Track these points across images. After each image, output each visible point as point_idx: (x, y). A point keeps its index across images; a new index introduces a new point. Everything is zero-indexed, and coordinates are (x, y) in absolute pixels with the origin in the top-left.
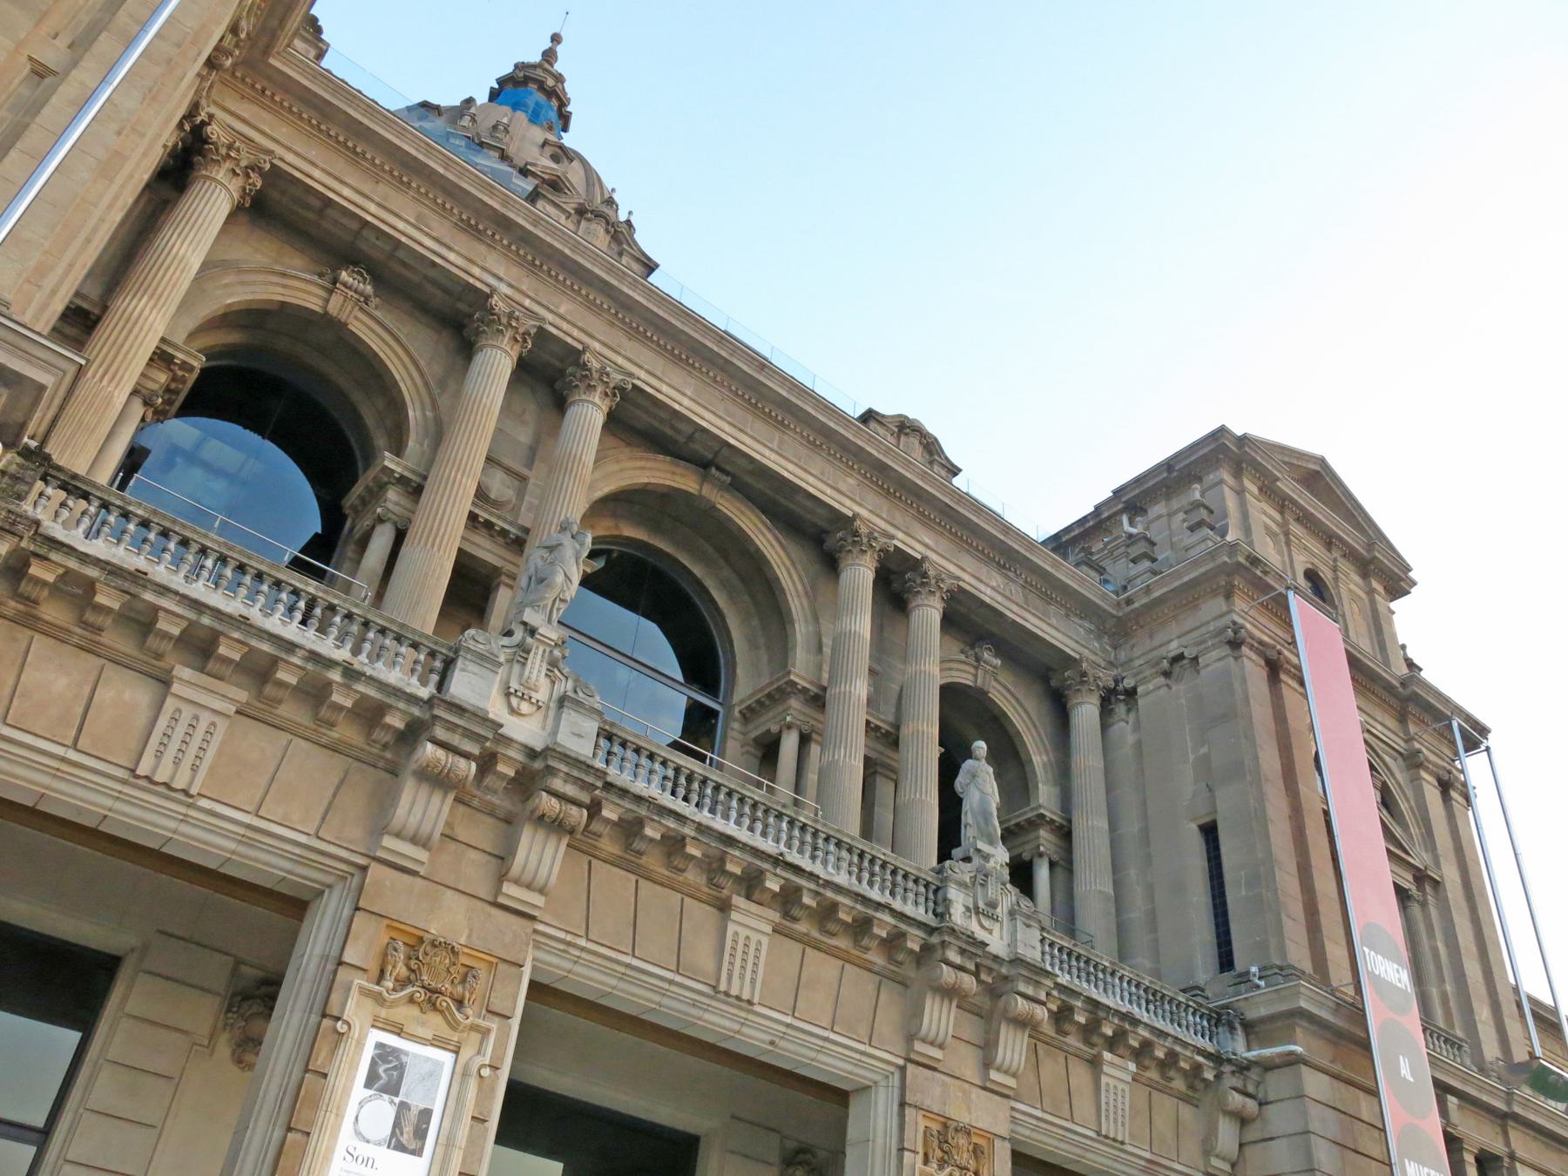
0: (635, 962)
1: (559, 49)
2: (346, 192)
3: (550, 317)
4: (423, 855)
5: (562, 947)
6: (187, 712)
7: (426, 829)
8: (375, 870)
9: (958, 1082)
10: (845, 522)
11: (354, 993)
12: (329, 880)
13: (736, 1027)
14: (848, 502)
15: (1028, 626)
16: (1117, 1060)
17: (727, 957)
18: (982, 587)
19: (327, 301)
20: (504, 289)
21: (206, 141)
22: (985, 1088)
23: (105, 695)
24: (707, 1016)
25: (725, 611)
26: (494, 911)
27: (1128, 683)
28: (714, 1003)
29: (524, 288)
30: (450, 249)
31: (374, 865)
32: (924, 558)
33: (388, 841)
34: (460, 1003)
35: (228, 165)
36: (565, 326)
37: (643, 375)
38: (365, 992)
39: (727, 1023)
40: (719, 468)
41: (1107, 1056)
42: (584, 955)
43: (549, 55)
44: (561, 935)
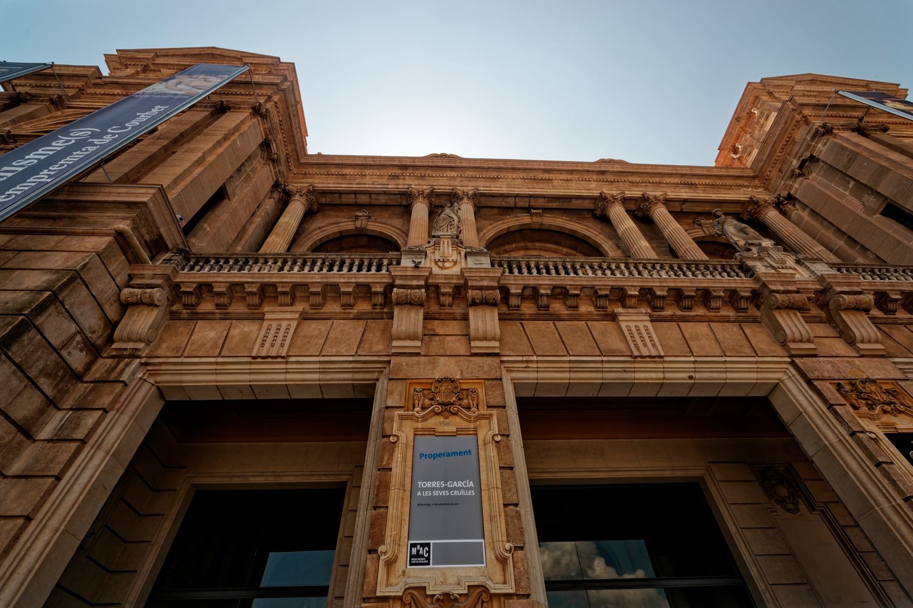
0: (572, 358)
4: (418, 343)
5: (524, 365)
6: (275, 325)
7: (411, 330)
8: (394, 360)
11: (396, 419)
12: (375, 376)
13: (661, 375)
17: (629, 338)
23: (235, 332)
24: (638, 375)
26: (472, 359)
27: (785, 193)
28: (637, 365)
33: (395, 343)
39: (654, 375)
42: (540, 365)
44: (520, 358)
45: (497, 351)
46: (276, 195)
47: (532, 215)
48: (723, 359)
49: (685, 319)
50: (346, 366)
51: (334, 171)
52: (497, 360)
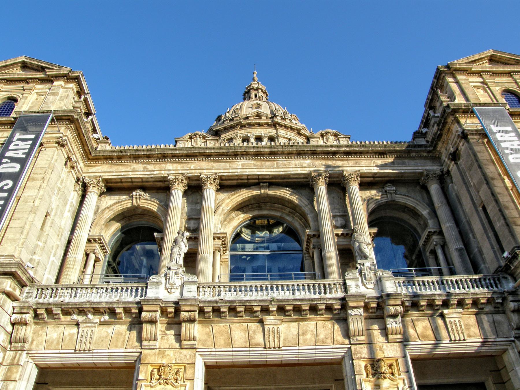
0: (234, 349)
6: (85, 329)
14: (308, 169)
16: (450, 311)
19: (132, 203)
27: (445, 170)
29: (179, 168)
30: (154, 171)
34: (176, 380)
36: (193, 171)
37: (222, 171)
38: (146, 386)
41: (445, 311)
44: (206, 350)
48: (314, 347)
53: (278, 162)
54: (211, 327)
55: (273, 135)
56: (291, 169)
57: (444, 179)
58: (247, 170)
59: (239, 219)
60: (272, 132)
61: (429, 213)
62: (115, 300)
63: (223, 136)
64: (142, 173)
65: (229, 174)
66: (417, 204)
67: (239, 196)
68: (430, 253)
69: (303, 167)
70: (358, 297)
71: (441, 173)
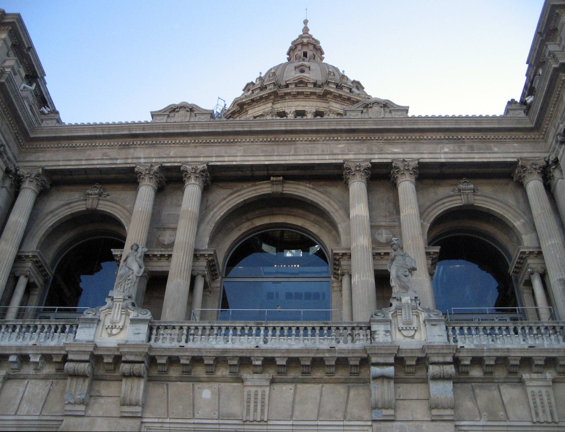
0: (196, 421)
1: (309, 25)
2: (73, 163)
3: (165, 160)
5: (160, 425)
9: (411, 423)
10: (339, 166)
14: (340, 157)
15: (476, 160)
16: (535, 376)
18: (438, 156)
20: (142, 161)
21: (19, 176)
22: (433, 421)
25: (319, 234)
27: (552, 158)
29: (153, 155)
30: (117, 159)
31: (65, 418)
32: (394, 160)
35: (28, 180)
37: (214, 159)
40: (274, 176)
41: (526, 376)
43: (306, 30)
44: (157, 420)
45: (140, 415)
46: (8, 183)
47: (273, 183)
48: (316, 423)
49: (303, 382)
50: (34, 423)
51: (65, 143)
52: (138, 422)
53: (298, 146)
54: (165, 387)
55: (321, 109)
56: (315, 157)
57: (550, 172)
58: (250, 158)
59: (240, 230)
60: (321, 105)
61: (524, 224)
62: (31, 343)
63: (250, 112)
64: (100, 162)
65: (224, 163)
66: (507, 211)
67: (239, 195)
68: (524, 285)
69: (333, 154)
70: (385, 349)
71: (545, 164)
